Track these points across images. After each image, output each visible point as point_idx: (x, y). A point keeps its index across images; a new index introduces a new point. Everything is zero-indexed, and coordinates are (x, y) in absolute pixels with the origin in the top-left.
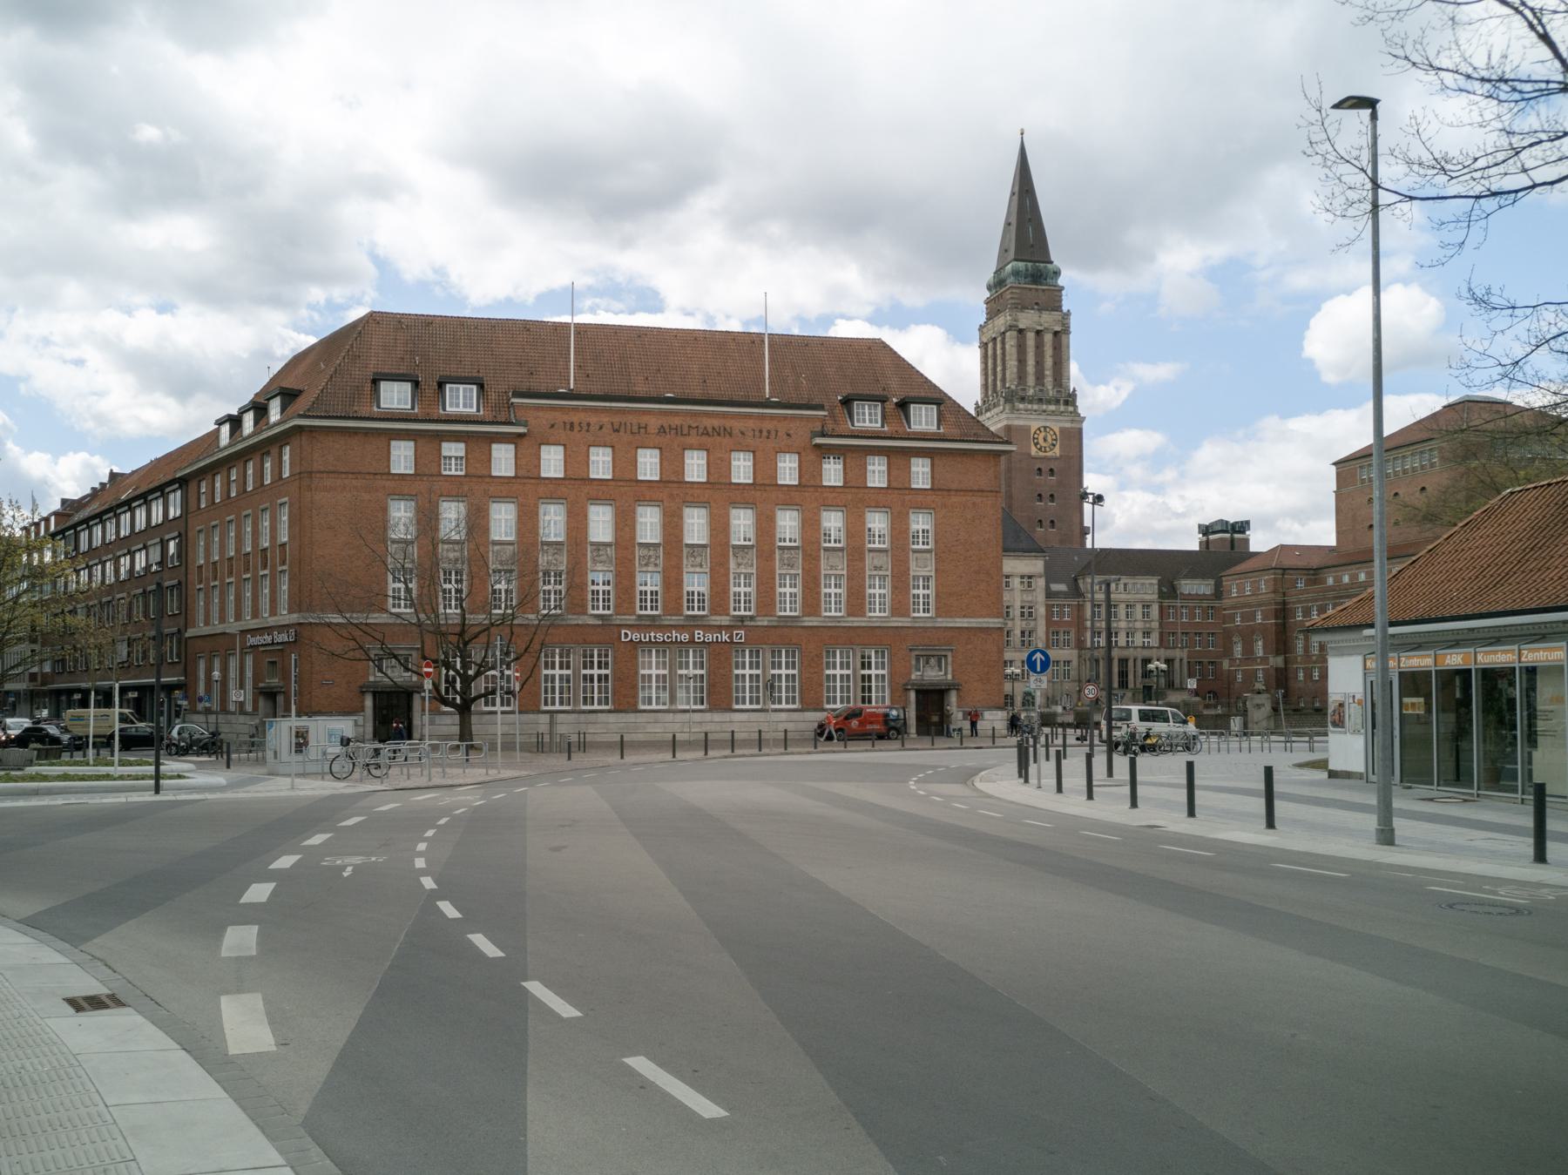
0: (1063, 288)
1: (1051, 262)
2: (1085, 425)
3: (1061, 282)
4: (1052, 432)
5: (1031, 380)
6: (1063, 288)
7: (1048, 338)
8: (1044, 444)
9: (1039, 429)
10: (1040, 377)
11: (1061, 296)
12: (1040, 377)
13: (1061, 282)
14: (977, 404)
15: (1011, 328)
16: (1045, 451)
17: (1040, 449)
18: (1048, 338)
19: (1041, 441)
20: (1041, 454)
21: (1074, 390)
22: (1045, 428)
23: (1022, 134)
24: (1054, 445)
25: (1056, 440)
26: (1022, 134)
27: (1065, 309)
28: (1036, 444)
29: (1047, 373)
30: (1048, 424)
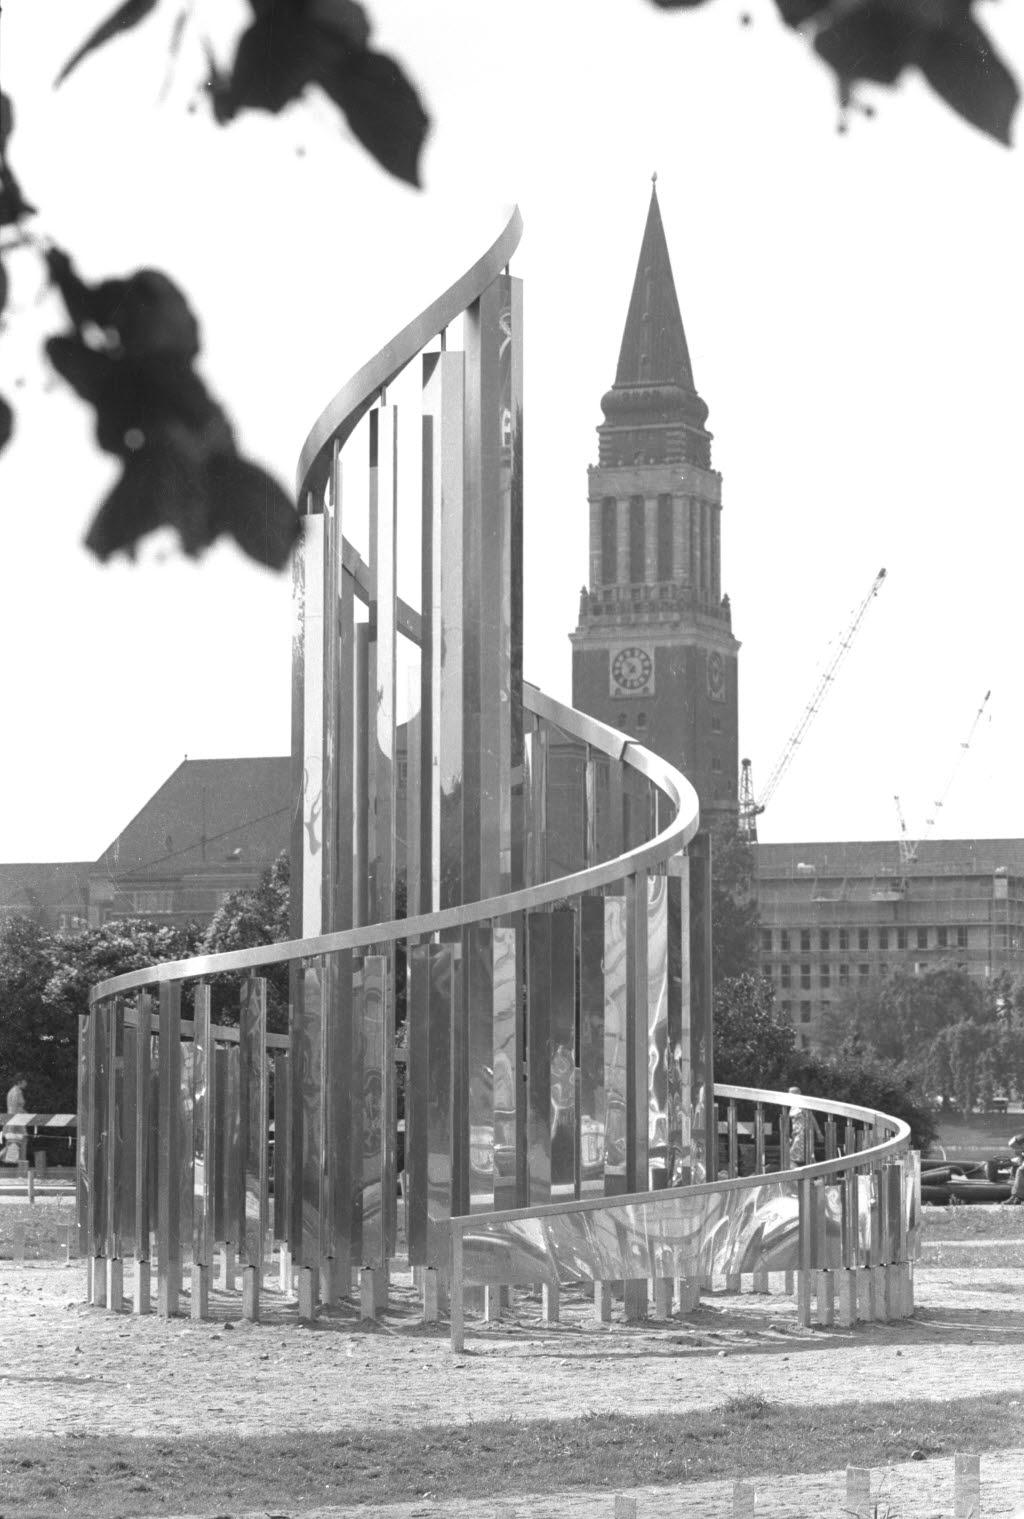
5: (622, 577)
7: (651, 507)
8: (633, 677)
9: (623, 653)
10: (636, 570)
12: (636, 570)
16: (632, 687)
17: (624, 684)
18: (651, 507)
19: (625, 671)
20: (627, 692)
22: (632, 650)
23: (654, 179)
24: (647, 678)
25: (650, 668)
26: (654, 179)
28: (617, 678)
29: (648, 561)
30: (630, 644)
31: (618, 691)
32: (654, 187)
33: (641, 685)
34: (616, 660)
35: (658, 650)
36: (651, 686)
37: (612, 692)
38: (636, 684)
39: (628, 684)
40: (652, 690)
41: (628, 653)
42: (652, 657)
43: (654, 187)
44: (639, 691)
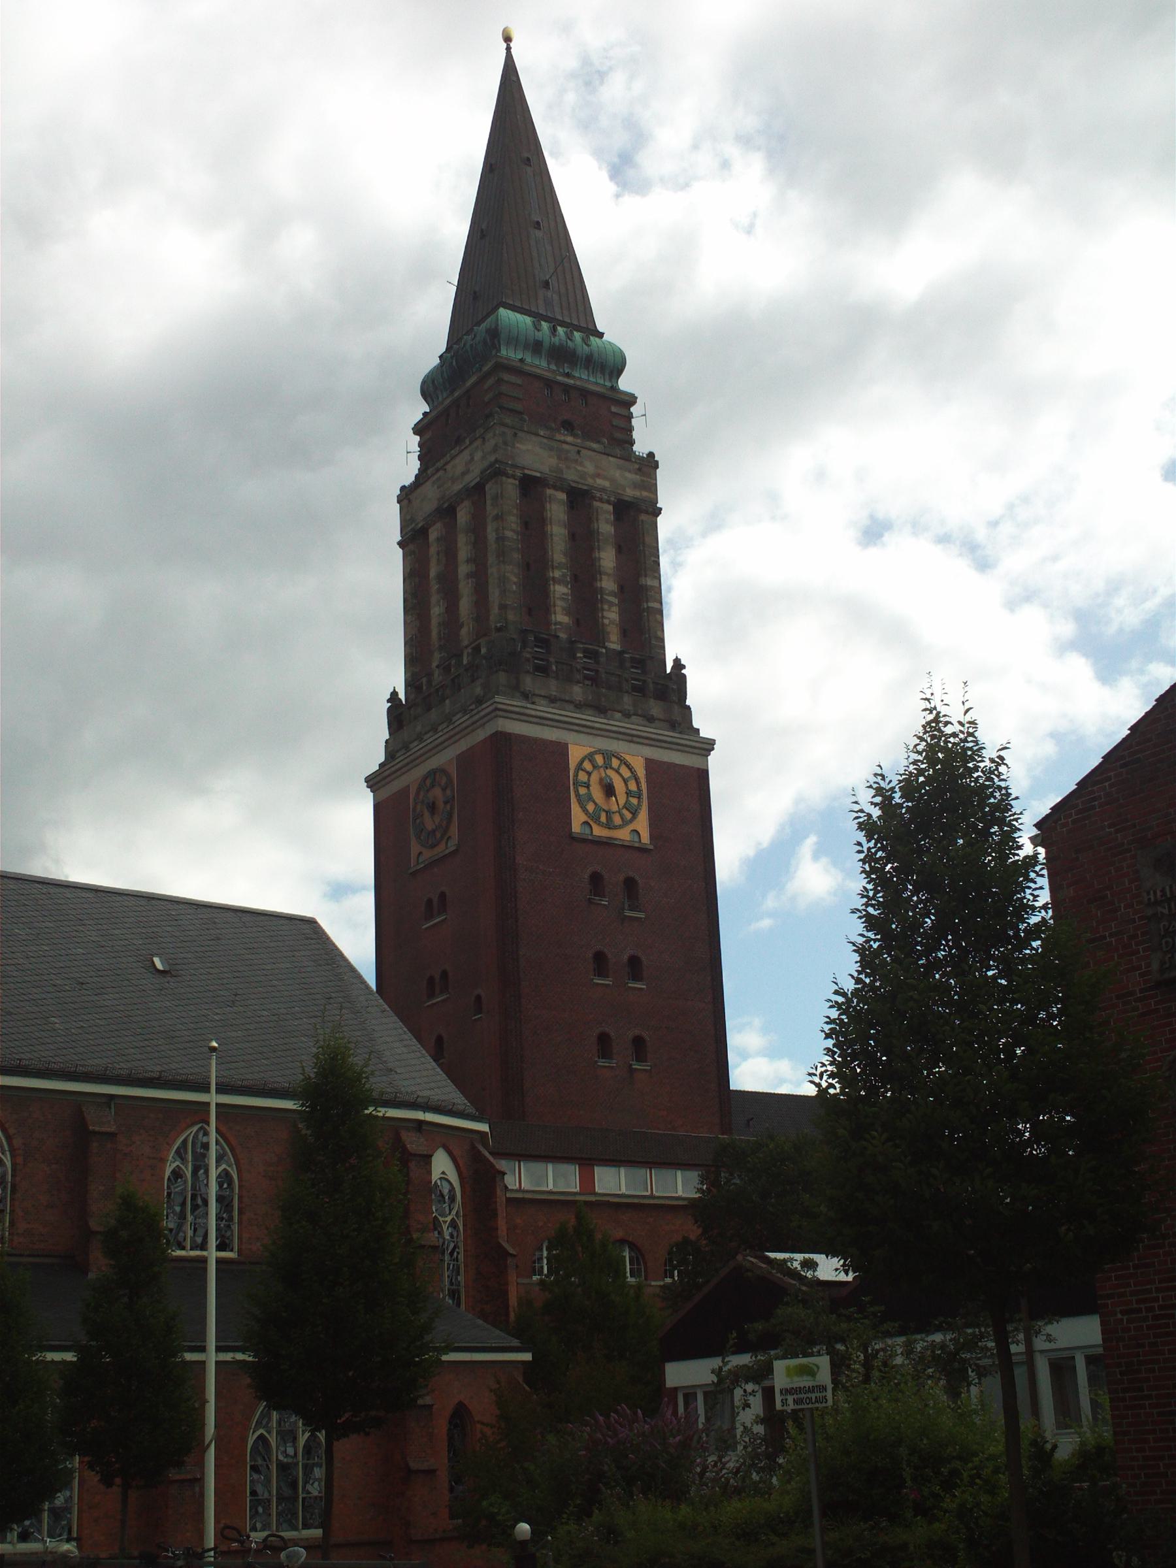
0: (631, 400)
1: (601, 335)
2: (714, 762)
3: (625, 383)
4: (626, 773)
6: (631, 400)
9: (590, 757)
11: (630, 417)
13: (625, 383)
14: (394, 694)
15: (495, 472)
20: (598, 831)
21: (678, 665)
22: (608, 756)
23: (508, 39)
26: (508, 39)
27: (641, 447)
31: (586, 823)
32: (508, 49)
33: (626, 823)
34: (579, 767)
35: (650, 764)
36: (642, 824)
37: (576, 827)
38: (617, 820)
39: (603, 819)
40: (645, 838)
41: (599, 760)
42: (641, 773)
43: (508, 49)
44: (624, 835)
